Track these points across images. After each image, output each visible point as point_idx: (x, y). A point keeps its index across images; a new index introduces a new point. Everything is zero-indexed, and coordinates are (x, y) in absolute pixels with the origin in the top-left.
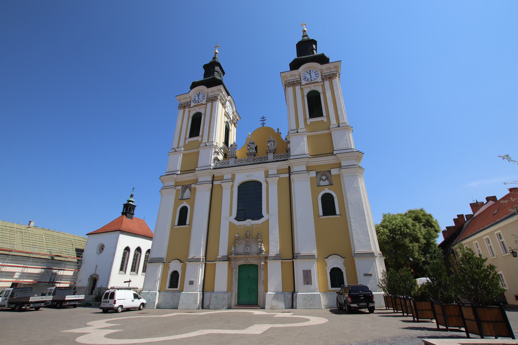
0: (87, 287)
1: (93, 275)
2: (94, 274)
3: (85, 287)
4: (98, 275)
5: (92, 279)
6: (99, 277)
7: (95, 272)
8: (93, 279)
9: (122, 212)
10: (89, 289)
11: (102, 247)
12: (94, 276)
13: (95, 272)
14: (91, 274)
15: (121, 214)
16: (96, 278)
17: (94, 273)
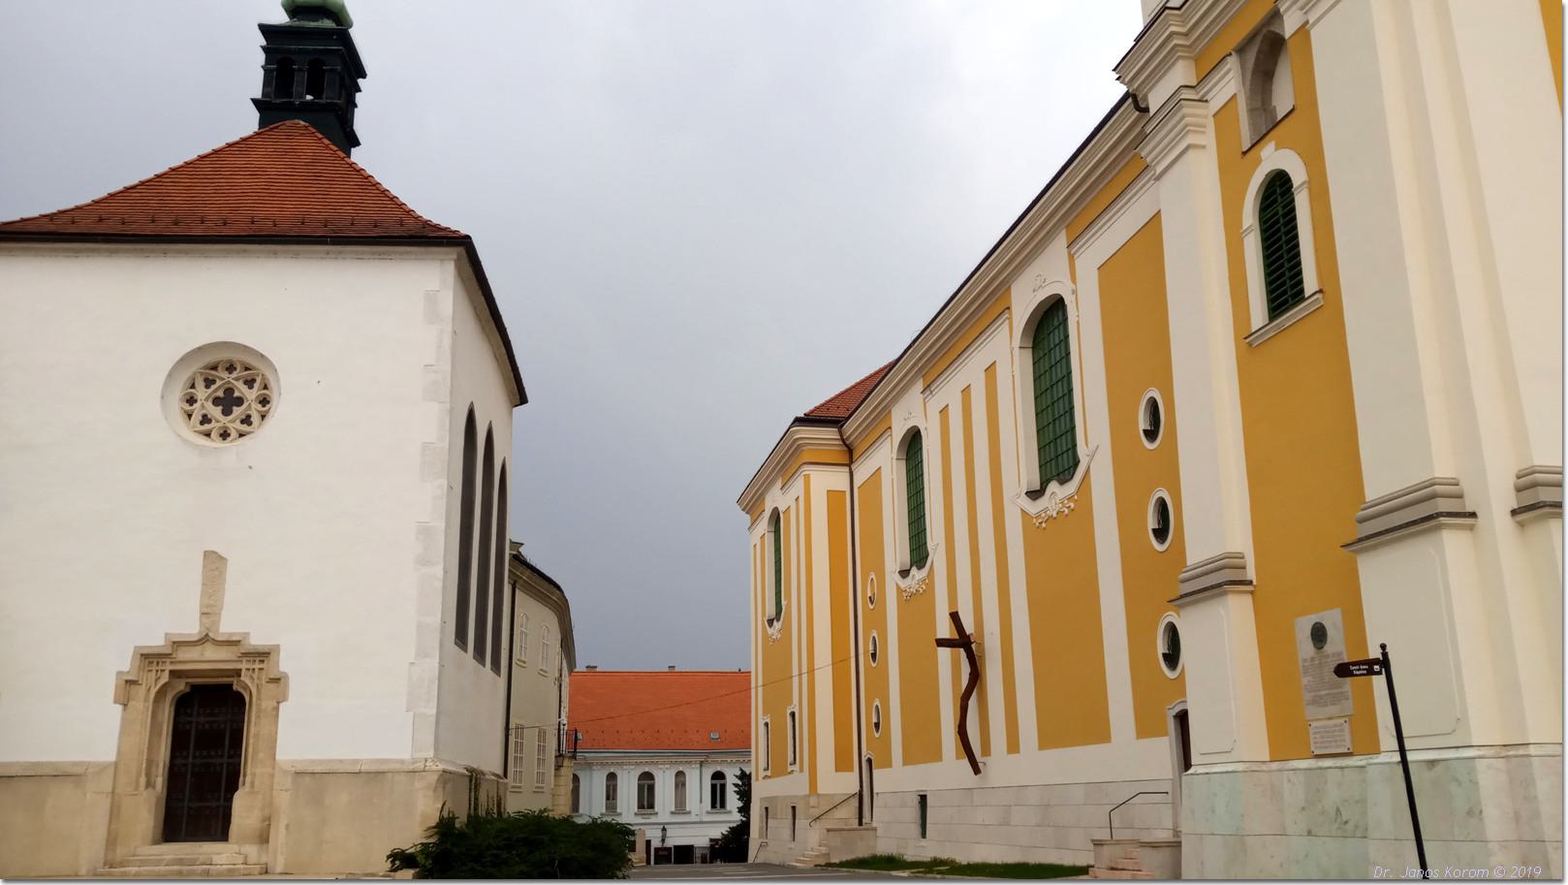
0: (116, 764)
1: (178, 644)
2: (205, 640)
3: (101, 768)
4: (257, 640)
5: (161, 693)
6: (285, 664)
7: (210, 612)
8: (181, 686)
9: (258, 95)
10: (149, 784)
11: (209, 383)
12: (209, 659)
13: (210, 612)
14: (156, 641)
15: (254, 116)
16: (238, 673)
17: (192, 629)
